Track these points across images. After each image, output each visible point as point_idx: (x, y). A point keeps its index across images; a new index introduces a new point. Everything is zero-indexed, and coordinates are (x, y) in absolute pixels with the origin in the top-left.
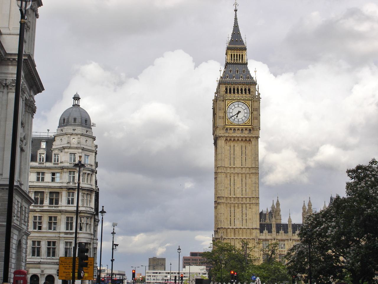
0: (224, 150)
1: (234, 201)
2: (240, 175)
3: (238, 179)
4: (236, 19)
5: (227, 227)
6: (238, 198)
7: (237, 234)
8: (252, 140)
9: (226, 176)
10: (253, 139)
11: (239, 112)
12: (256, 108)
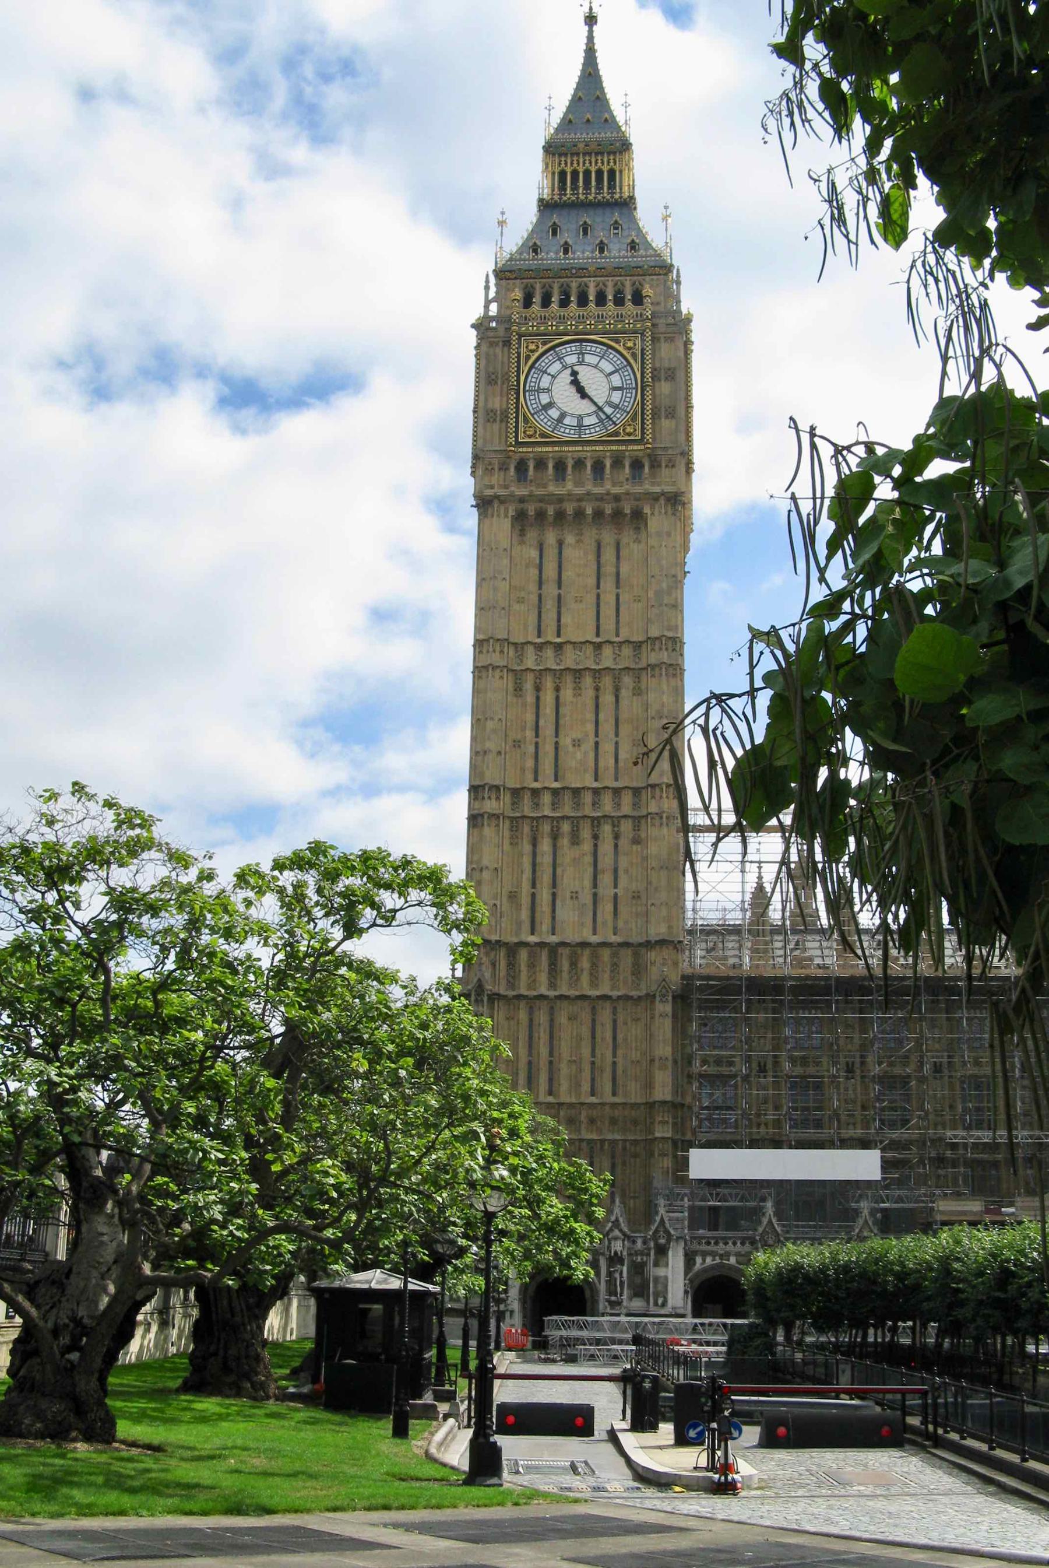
0: (506, 562)
1: (554, 806)
2: (588, 681)
3: (577, 704)
4: (590, 53)
6: (576, 792)
7: (565, 975)
8: (647, 510)
9: (518, 690)
10: (652, 508)
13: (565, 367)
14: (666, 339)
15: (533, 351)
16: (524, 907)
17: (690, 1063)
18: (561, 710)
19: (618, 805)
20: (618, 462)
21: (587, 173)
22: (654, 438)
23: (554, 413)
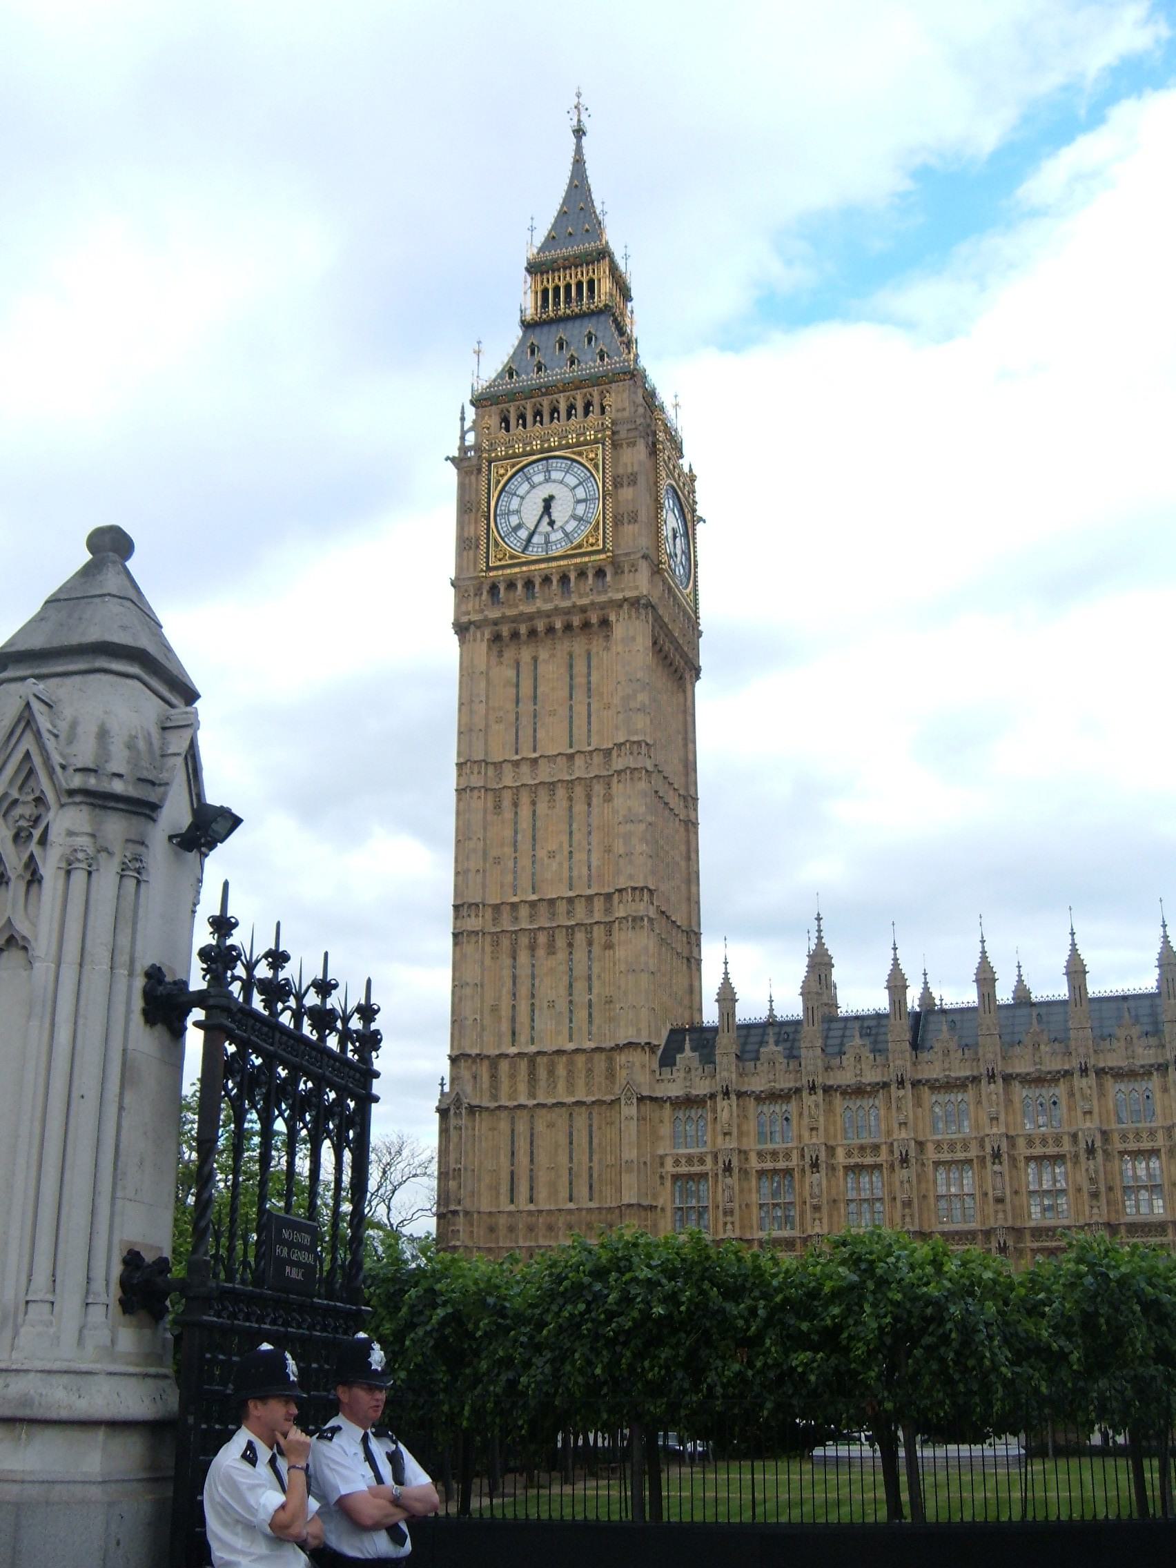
0: (483, 684)
1: (532, 918)
3: (552, 814)
5: (494, 1052)
6: (552, 902)
8: (612, 618)
9: (498, 807)
11: (548, 502)
12: (630, 470)
13: (533, 487)
14: (628, 445)
15: (502, 476)
16: (504, 1020)
17: (662, 1165)
18: (538, 824)
20: (582, 574)
21: (568, 287)
22: (616, 544)
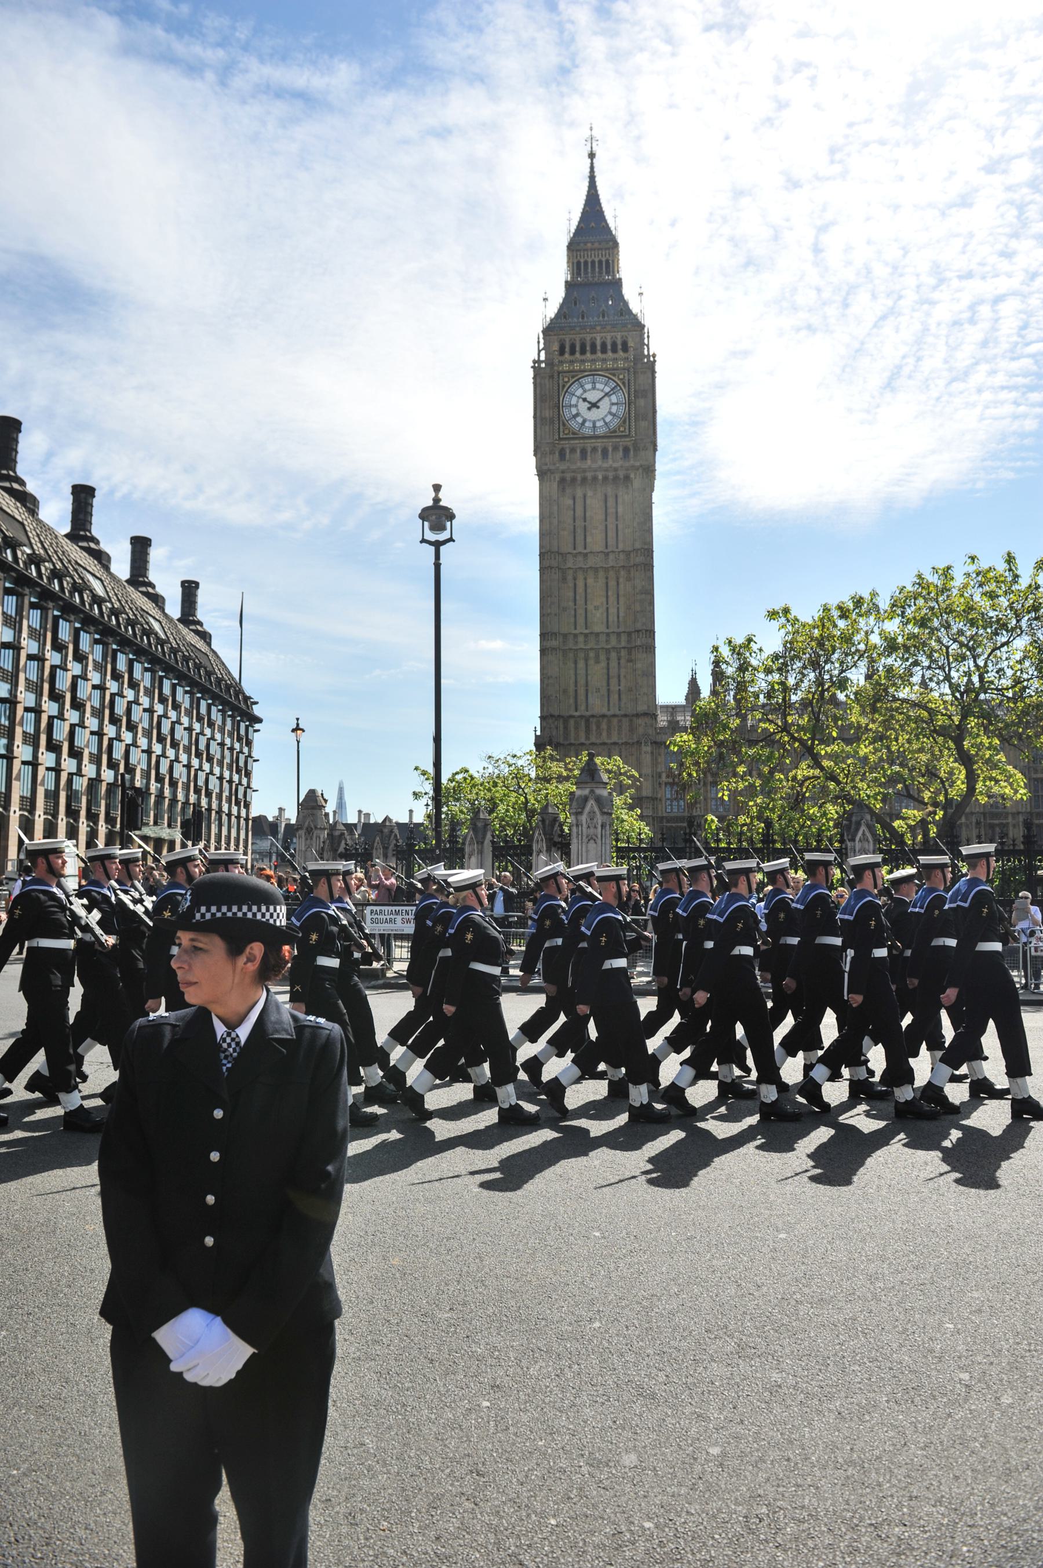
0: (556, 508)
2: (601, 574)
5: (565, 714)
6: (597, 634)
8: (632, 476)
17: (660, 777)
19: (619, 641)
20: (615, 448)
23: (580, 420)
